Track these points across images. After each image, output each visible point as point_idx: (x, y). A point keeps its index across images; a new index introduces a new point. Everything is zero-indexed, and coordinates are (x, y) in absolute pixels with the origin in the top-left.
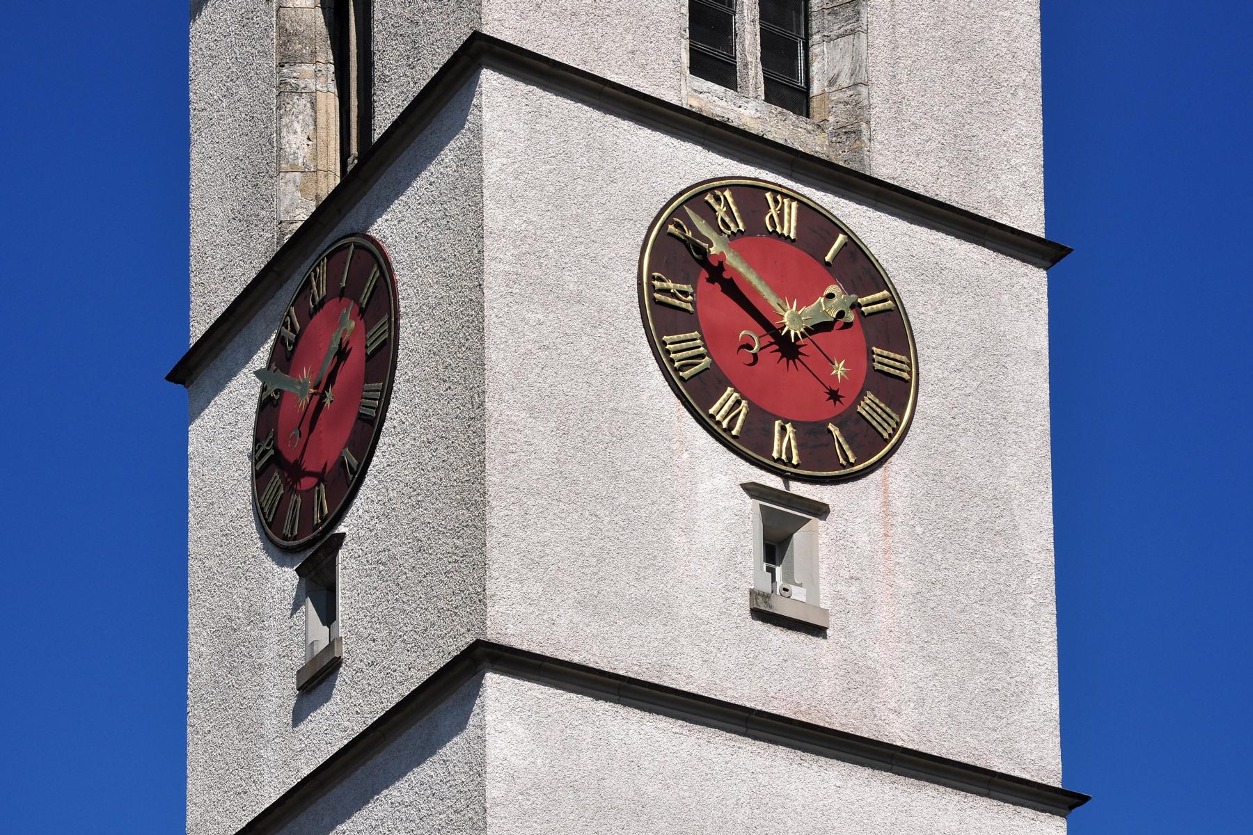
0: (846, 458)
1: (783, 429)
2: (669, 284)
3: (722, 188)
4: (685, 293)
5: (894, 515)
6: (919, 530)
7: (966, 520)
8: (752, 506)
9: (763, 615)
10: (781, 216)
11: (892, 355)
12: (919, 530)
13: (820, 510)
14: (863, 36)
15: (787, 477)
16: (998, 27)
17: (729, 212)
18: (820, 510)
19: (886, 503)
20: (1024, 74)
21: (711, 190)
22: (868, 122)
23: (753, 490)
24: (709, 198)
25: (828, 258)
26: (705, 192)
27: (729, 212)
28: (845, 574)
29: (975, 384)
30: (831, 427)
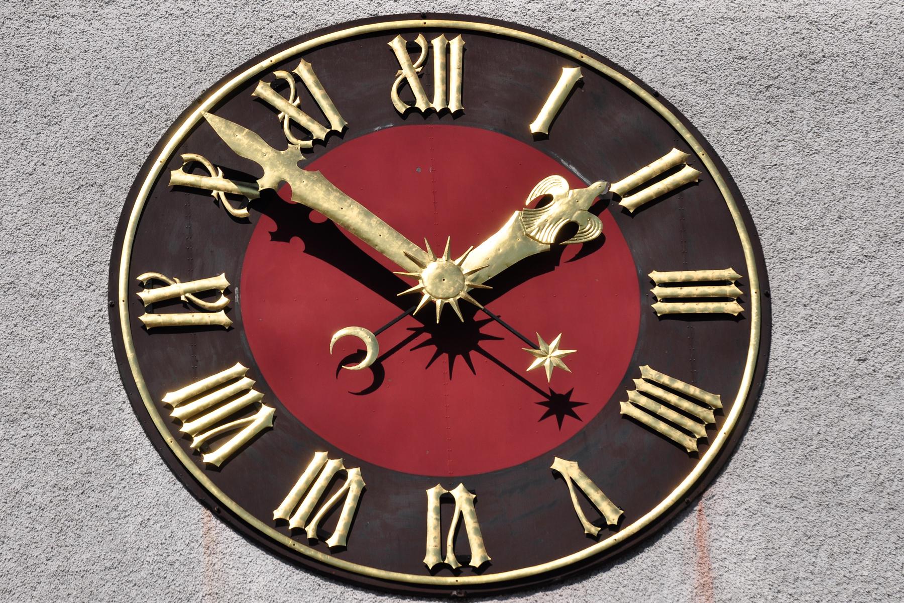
0: (599, 519)
1: (447, 501)
3: (289, 63)
4: (211, 294)
26: (252, 81)
30: (559, 464)
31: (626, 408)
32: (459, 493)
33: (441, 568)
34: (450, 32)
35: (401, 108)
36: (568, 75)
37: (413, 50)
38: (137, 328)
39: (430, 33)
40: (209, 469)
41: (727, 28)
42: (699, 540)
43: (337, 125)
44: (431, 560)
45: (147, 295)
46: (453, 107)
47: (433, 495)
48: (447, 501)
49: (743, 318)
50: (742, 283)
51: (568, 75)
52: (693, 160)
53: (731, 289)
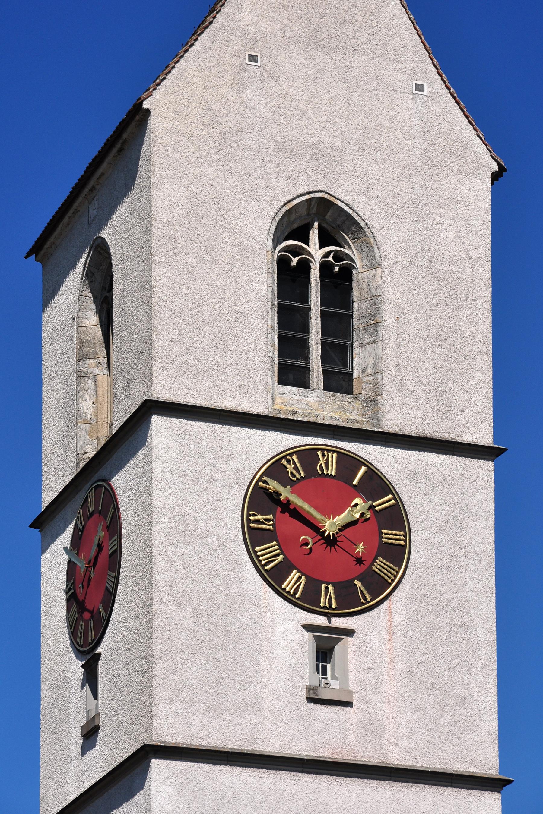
0: (365, 599)
1: (327, 588)
2: (260, 517)
3: (291, 454)
5: (395, 626)
6: (410, 633)
7: (440, 622)
8: (308, 636)
9: (311, 700)
10: (327, 464)
11: (394, 532)
12: (410, 633)
13: (349, 633)
14: (379, 344)
15: (329, 616)
16: (465, 320)
17: (296, 468)
18: (349, 633)
19: (390, 621)
20: (480, 345)
21: (284, 457)
22: (382, 395)
23: (308, 628)
24: (284, 462)
25: (355, 483)
26: (281, 459)
27: (296, 468)
28: (365, 667)
29: (447, 539)
30: (356, 582)
31: (373, 568)
32: (330, 586)
33: (325, 607)
34: (334, 451)
35: (320, 472)
36: (363, 469)
37: (324, 455)
38: (249, 527)
39: (329, 451)
40: (266, 570)
41: (405, 461)
42: (390, 611)
43: (303, 475)
44: (322, 605)
45: (252, 518)
46: (333, 474)
47: (323, 586)
48: (327, 588)
49: (405, 546)
50: (405, 536)
51: (363, 469)
52: (394, 498)
53: (402, 537)
